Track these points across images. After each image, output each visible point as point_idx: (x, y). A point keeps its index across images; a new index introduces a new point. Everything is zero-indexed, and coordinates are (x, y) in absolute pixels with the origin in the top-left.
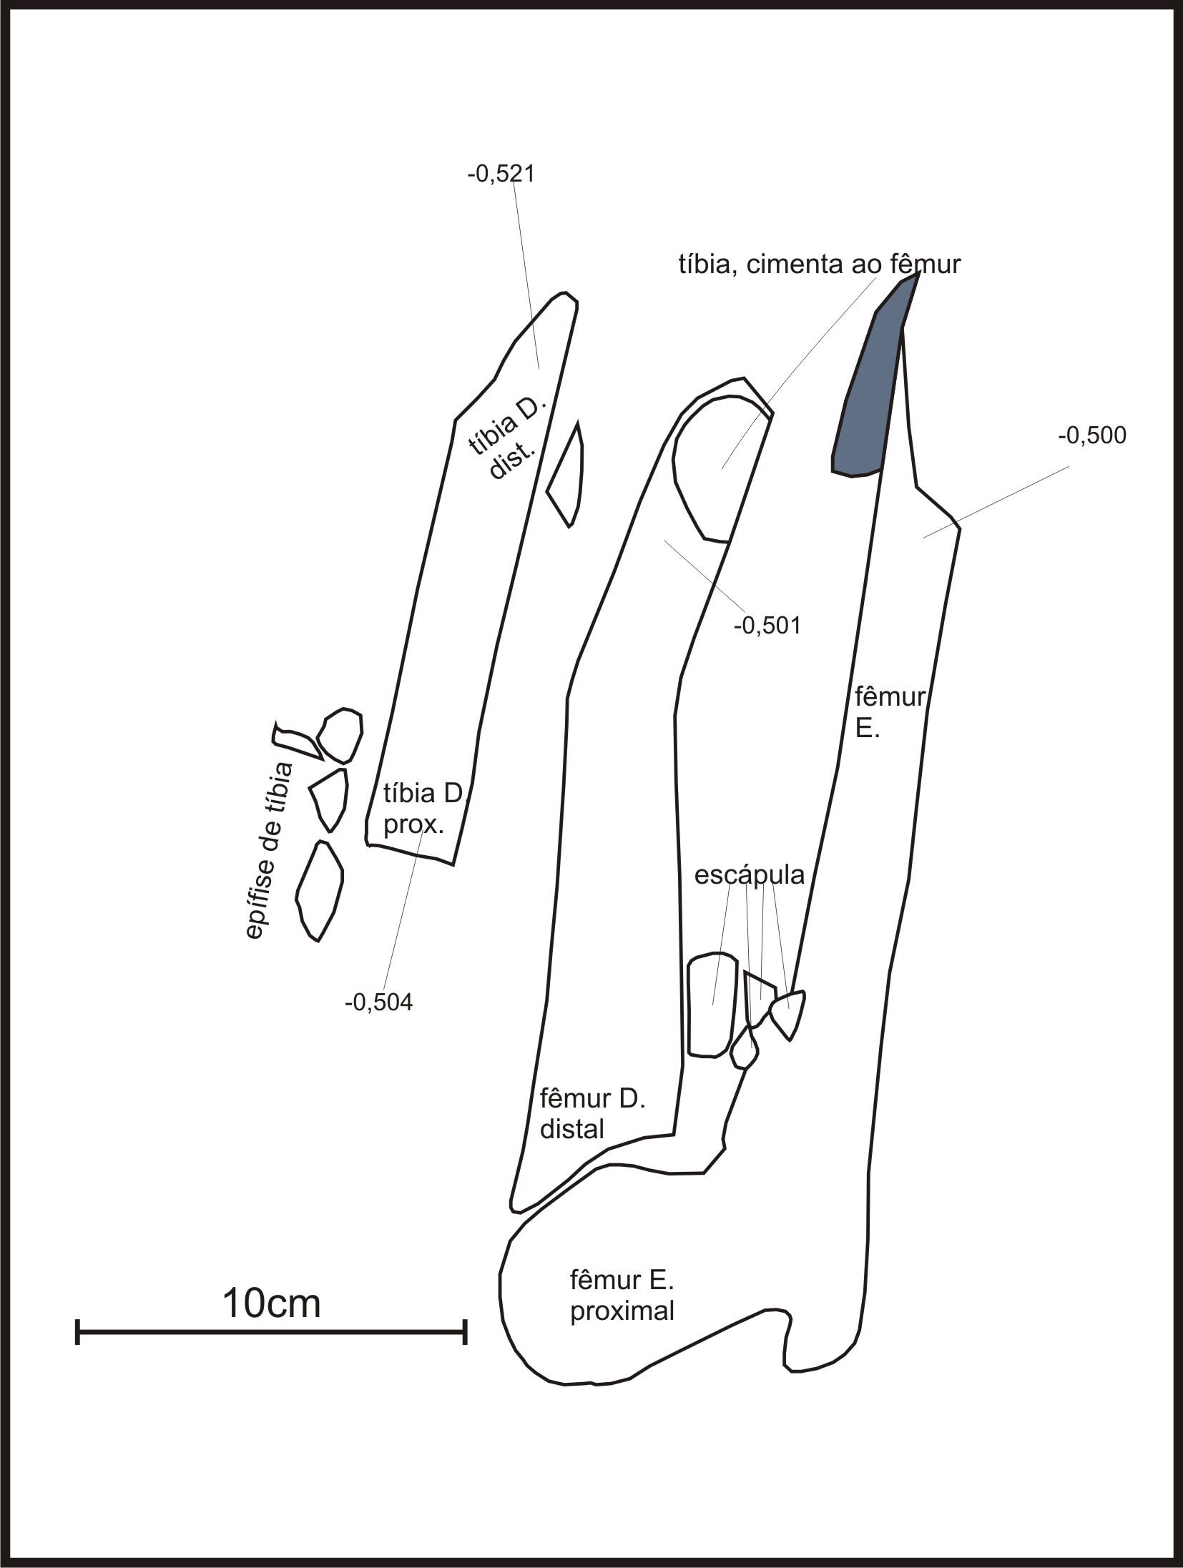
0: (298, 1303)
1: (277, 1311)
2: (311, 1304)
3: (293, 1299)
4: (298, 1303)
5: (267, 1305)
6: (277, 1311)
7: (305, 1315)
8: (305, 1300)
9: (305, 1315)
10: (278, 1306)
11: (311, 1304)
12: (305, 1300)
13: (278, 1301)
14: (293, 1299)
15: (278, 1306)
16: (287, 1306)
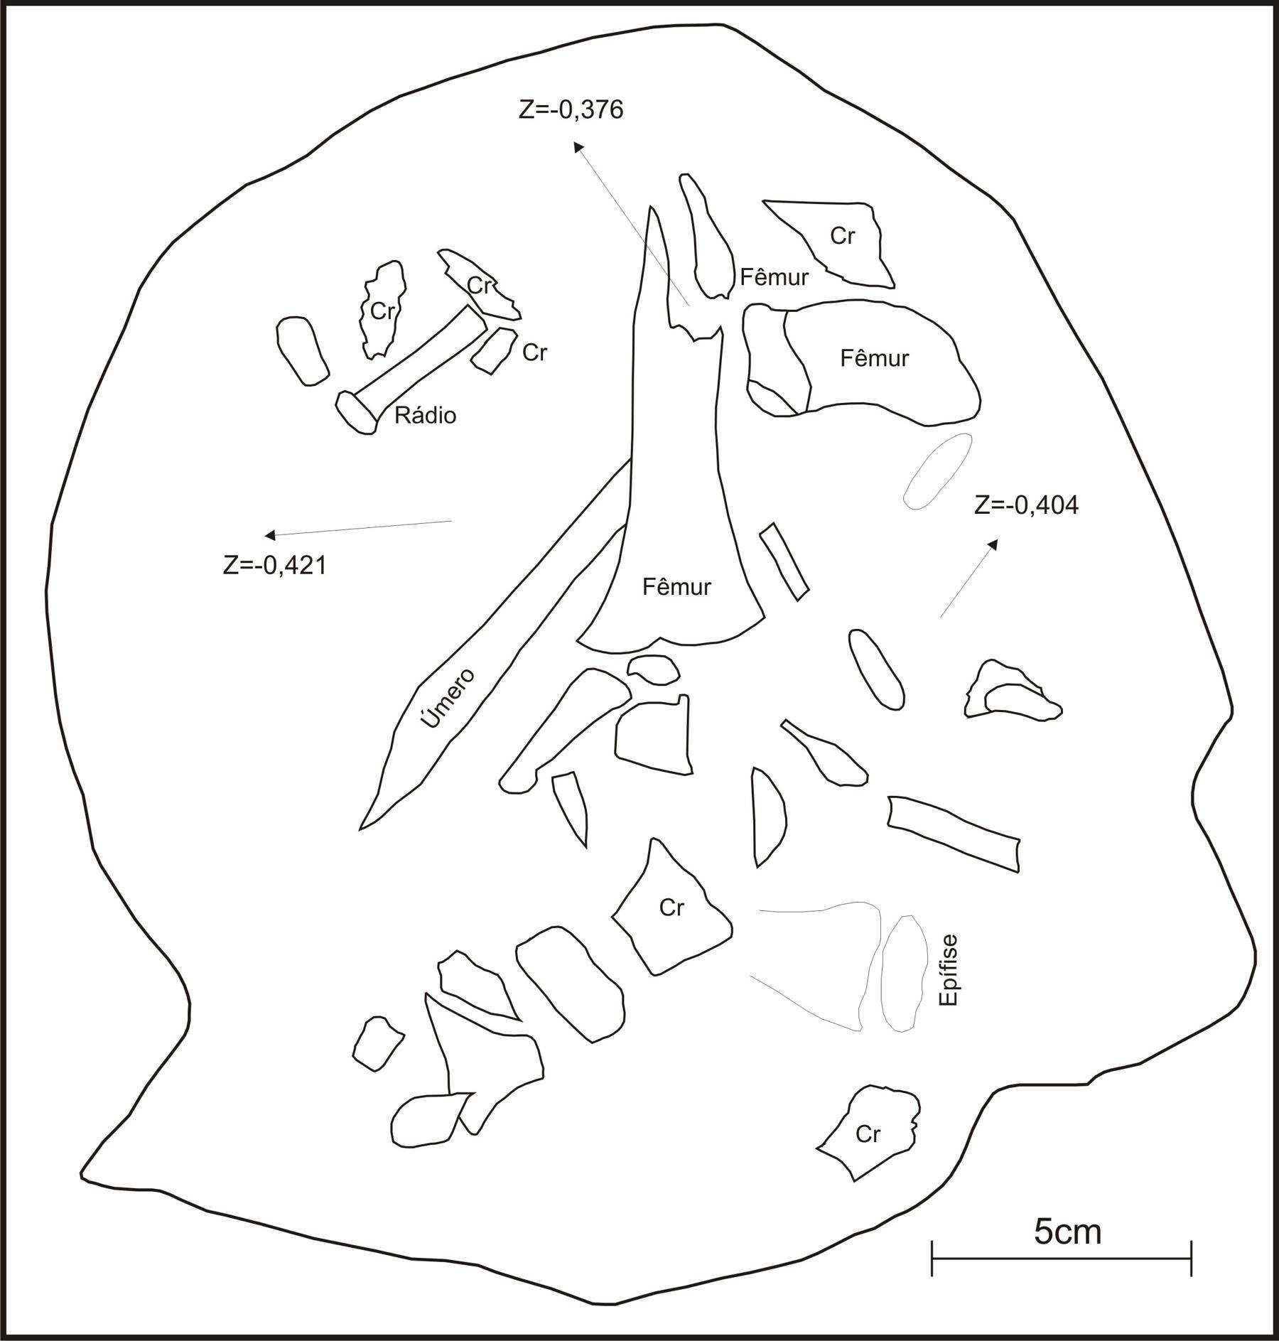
0: (1082, 1231)
1: (1064, 1239)
2: (1093, 1231)
3: (1077, 1228)
4: (1082, 1231)
5: (1054, 1235)
6: (1063, 1237)
7: (1088, 1242)
8: (1088, 1229)
9: (1088, 1242)
10: (1064, 1234)
11: (1093, 1231)
12: (1088, 1229)
13: (1063, 1230)
14: (1077, 1228)
15: (1064, 1234)
16: (1072, 1234)
